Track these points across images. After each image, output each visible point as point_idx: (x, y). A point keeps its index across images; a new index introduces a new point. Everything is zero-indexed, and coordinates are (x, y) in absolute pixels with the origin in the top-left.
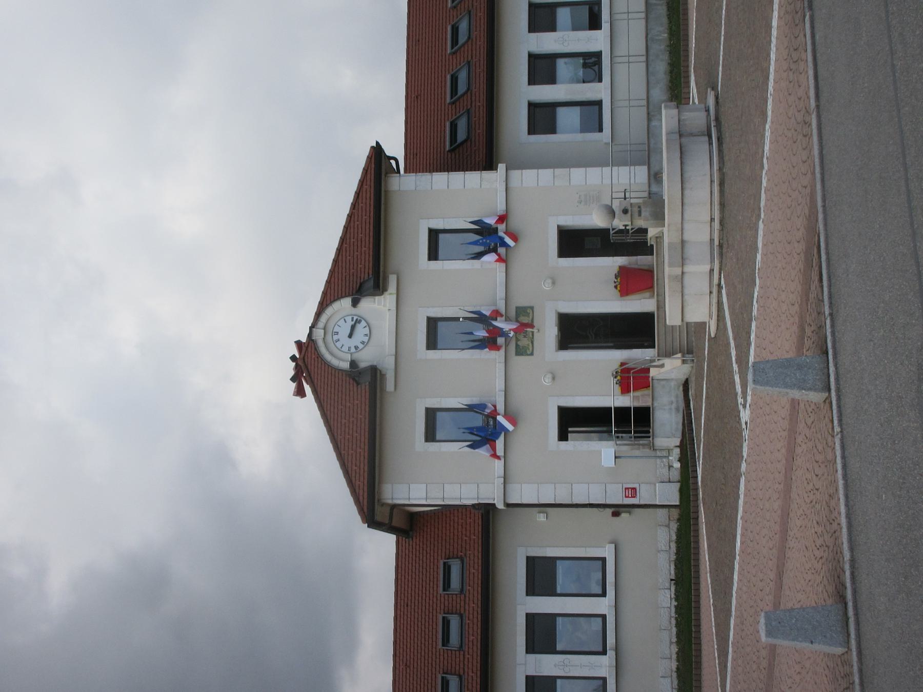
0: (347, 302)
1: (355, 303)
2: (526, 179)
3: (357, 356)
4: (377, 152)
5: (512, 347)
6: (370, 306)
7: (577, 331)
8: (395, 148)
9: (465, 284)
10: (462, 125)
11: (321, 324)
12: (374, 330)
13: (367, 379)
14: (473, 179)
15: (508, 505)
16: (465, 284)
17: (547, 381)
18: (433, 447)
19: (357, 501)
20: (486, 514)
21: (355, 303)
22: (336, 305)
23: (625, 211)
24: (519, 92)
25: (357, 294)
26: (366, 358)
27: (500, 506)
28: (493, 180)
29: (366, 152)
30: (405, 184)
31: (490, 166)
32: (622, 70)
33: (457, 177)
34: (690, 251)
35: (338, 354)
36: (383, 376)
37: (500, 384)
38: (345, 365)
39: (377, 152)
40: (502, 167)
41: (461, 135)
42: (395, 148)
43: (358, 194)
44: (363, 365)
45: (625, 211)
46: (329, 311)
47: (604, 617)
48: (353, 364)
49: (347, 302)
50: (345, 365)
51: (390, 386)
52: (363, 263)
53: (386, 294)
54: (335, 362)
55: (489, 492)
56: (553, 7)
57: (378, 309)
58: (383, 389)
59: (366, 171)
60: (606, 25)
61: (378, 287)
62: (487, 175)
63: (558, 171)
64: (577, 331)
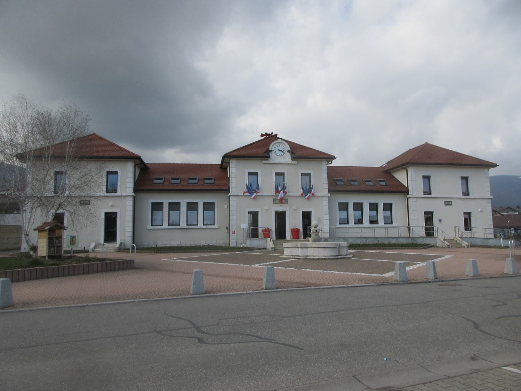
0: (289, 149)
1: (289, 151)
2: (325, 202)
4: (333, 158)
5: (275, 198)
6: (288, 155)
7: (281, 217)
8: (335, 163)
9: (294, 184)
10: (342, 183)
11: (282, 141)
12: (280, 157)
13: (266, 155)
15: (229, 197)
16: (294, 184)
17: (266, 208)
19: (230, 152)
20: (227, 190)
21: (289, 151)
22: (288, 146)
23: (316, 231)
24: (351, 200)
25: (291, 152)
26: (272, 155)
27: (229, 194)
28: (325, 192)
29: (333, 155)
30: (324, 166)
31: (330, 191)
32: (358, 230)
33: (326, 181)
34: (305, 250)
35: (273, 147)
37: (265, 194)
38: (270, 149)
39: (333, 158)
40: (329, 195)
41: (338, 183)
42: (335, 163)
44: (270, 154)
45: (316, 231)
46: (286, 144)
47: (197, 225)
48: (271, 151)
49: (289, 149)
50: (270, 149)
51: (264, 162)
52: (300, 153)
53: (291, 161)
54: (271, 145)
55: (233, 192)
56: (391, 211)
57: (287, 158)
59: (328, 154)
60: (371, 225)
61: (293, 158)
63: (328, 211)
64: (281, 217)
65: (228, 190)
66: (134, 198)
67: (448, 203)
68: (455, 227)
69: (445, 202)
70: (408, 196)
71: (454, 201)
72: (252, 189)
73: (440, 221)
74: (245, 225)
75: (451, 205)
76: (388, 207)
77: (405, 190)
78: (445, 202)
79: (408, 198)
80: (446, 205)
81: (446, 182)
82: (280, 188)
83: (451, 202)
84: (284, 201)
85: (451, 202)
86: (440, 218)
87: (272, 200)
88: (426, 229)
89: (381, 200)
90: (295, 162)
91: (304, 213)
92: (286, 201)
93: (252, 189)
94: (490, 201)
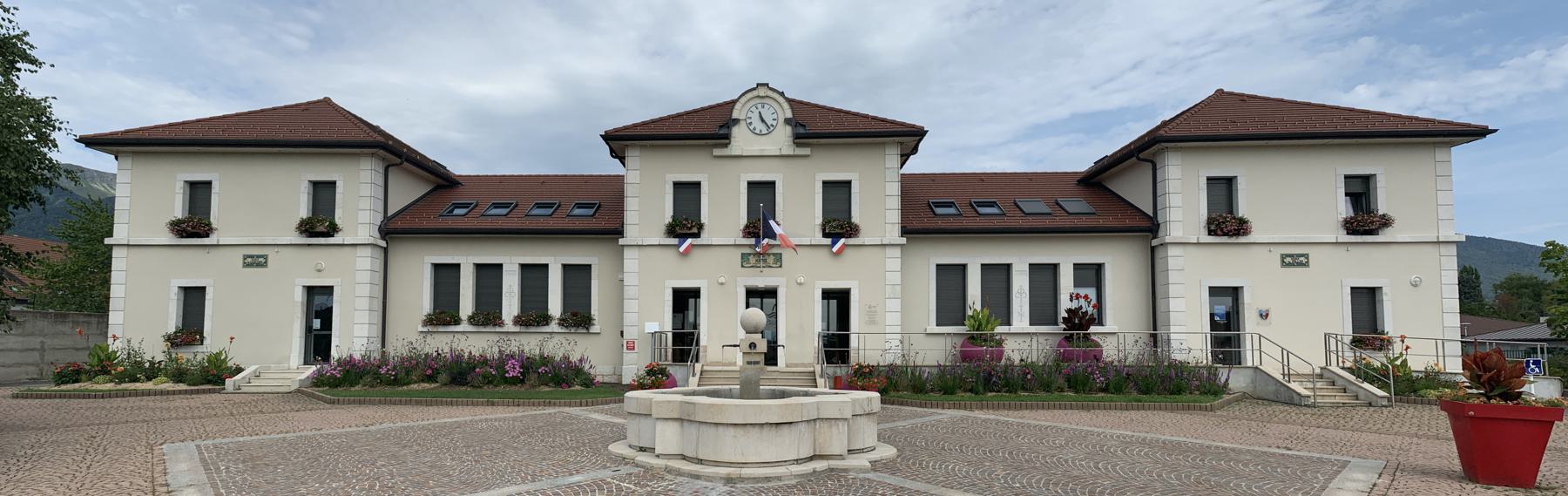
0: (789, 115)
1: (787, 121)
3: (743, 124)
5: (748, 251)
6: (784, 134)
11: (770, 93)
14: (894, 217)
17: (722, 280)
18: (670, 190)
21: (787, 121)
22: (786, 105)
27: (621, 242)
28: (893, 234)
31: (905, 232)
33: (895, 203)
36: (726, 145)
38: (735, 115)
40: (903, 241)
43: (884, 120)
48: (736, 121)
49: (789, 115)
50: (735, 115)
51: (717, 152)
55: (632, 234)
57: (781, 139)
58: (716, 146)
59: (903, 124)
60: (1034, 329)
61: (800, 138)
62: (897, 229)
63: (898, 288)
65: (619, 232)
66: (386, 250)
67: (1295, 261)
68: (1327, 336)
69: (1283, 257)
70: (1155, 242)
71: (1313, 252)
72: (685, 226)
73: (1264, 315)
74: (662, 321)
75: (1306, 265)
76: (1091, 275)
77: (1146, 224)
78: (1283, 257)
79: (1153, 249)
80: (1284, 264)
81: (1293, 197)
82: (759, 226)
83: (1306, 256)
84: (771, 260)
85: (1306, 256)
86: (1264, 308)
87: (737, 253)
88: (1218, 342)
89: (1066, 257)
90: (807, 151)
91: (827, 294)
92: (779, 258)
93: (685, 226)
94: (1453, 250)
